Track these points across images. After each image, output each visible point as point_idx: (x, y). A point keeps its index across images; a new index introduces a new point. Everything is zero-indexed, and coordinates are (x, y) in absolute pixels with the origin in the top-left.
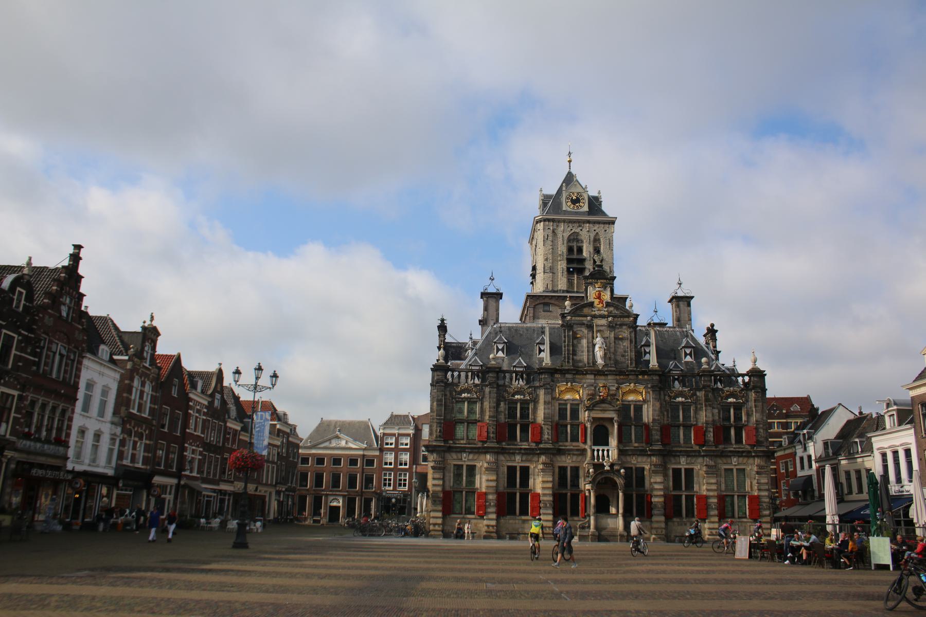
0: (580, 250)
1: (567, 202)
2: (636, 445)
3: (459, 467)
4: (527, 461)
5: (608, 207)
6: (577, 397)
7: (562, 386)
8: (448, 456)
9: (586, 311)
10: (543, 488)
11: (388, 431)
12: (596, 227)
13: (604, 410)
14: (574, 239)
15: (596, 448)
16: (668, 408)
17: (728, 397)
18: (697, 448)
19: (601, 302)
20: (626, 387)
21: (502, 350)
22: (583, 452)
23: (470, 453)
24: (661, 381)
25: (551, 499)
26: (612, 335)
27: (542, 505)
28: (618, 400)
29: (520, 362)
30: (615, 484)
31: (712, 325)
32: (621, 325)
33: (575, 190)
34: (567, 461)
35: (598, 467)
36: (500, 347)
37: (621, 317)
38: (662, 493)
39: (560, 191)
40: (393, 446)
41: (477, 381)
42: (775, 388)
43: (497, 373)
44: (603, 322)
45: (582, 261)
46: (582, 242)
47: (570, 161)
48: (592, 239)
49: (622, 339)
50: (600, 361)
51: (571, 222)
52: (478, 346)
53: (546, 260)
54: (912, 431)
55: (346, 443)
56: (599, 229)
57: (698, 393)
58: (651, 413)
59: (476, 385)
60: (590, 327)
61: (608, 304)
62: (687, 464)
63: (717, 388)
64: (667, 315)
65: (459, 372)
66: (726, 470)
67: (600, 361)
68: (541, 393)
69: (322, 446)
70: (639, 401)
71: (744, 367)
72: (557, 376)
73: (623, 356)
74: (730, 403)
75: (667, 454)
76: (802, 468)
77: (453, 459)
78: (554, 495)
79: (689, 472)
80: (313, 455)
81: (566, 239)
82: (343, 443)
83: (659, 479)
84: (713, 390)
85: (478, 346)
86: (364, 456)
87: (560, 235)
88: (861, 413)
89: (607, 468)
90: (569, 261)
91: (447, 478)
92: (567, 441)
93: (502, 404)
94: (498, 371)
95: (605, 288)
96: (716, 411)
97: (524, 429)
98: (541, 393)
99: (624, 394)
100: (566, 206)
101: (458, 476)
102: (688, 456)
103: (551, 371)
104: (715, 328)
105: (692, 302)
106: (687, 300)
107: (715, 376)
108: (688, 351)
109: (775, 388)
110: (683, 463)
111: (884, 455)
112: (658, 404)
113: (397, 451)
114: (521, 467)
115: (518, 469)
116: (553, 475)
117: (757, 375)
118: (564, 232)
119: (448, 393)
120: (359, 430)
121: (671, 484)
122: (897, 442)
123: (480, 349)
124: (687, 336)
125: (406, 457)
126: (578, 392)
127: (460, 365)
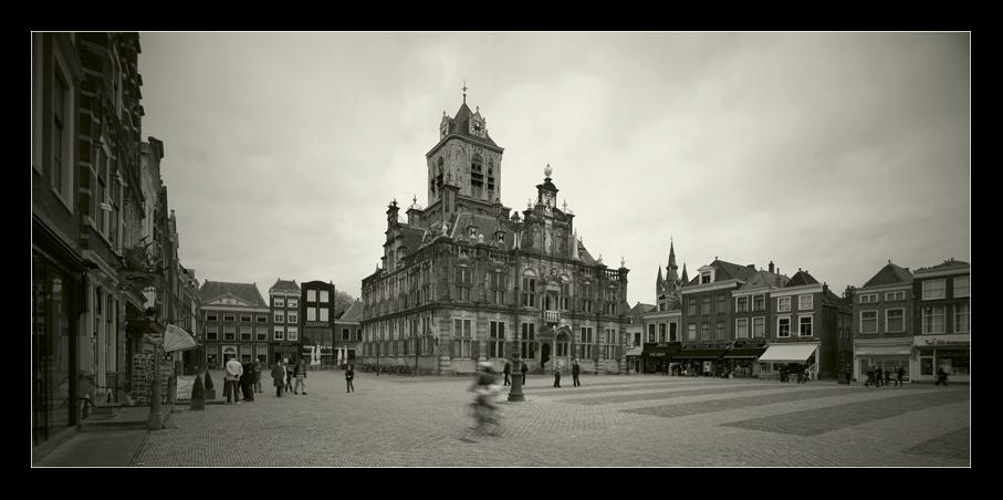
0: (479, 168)
3: (458, 322)
8: (451, 312)
13: (554, 285)
32: (560, 226)
34: (528, 320)
44: (548, 222)
45: (481, 177)
46: (481, 162)
50: (549, 252)
90: (473, 175)
92: (526, 304)
100: (472, 131)
101: (458, 327)
103: (521, 253)
110: (587, 324)
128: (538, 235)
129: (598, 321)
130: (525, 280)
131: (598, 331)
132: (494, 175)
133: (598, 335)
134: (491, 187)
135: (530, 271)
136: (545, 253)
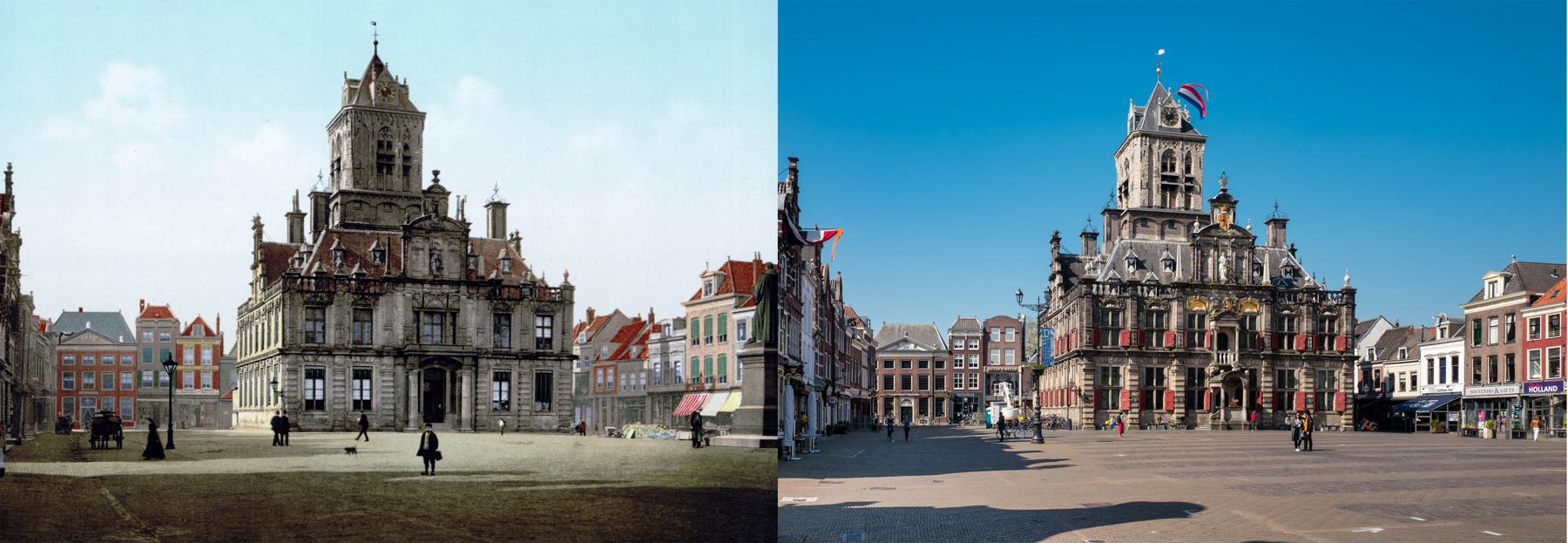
0: (1173, 168)
3: (1105, 369)
9: (1213, 232)
16: (1277, 320)
34: (1196, 363)
45: (1174, 178)
50: (1223, 277)
60: (1216, 247)
61: (1232, 227)
68: (1175, 305)
75: (1274, 358)
77: (1100, 363)
87: (1155, 151)
90: (1164, 178)
94: (1134, 284)
98: (1175, 305)
111: (1431, 361)
118: (1159, 148)
125: (976, 360)
134: (1189, 189)
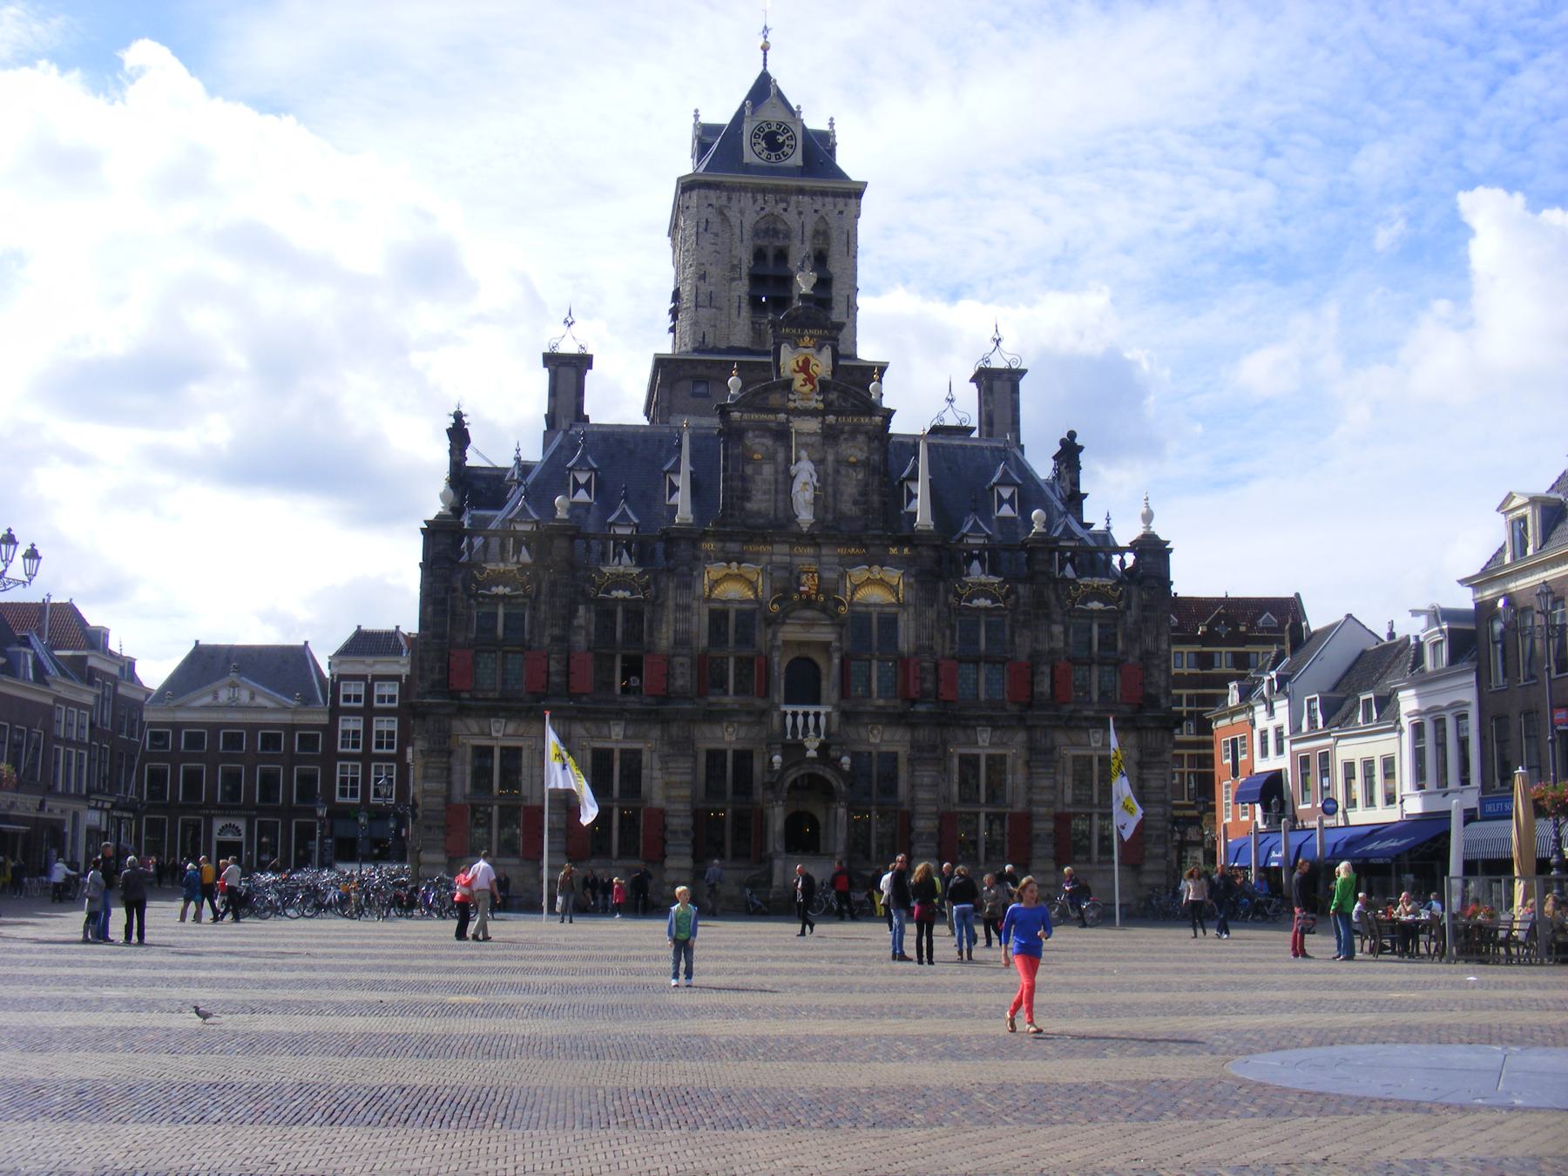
0: (782, 256)
1: (753, 145)
2: (881, 702)
3: (483, 753)
4: (635, 737)
5: (848, 160)
6: (750, 595)
7: (715, 571)
8: (457, 725)
9: (775, 399)
10: (668, 799)
11: (348, 669)
12: (819, 200)
13: (810, 624)
14: (767, 232)
15: (789, 709)
17: (1085, 601)
18: (1013, 709)
19: (810, 379)
20: (859, 574)
21: (587, 486)
22: (762, 715)
23: (509, 719)
24: (936, 563)
25: (690, 821)
26: (830, 458)
27: (668, 836)
28: (842, 603)
29: (624, 516)
30: (828, 793)
31: (1072, 435)
32: (855, 431)
33: (770, 114)
34: (728, 737)
35: (794, 750)
36: (582, 478)
37: (853, 414)
38: (934, 809)
39: (739, 117)
40: (361, 705)
41: (525, 557)
42: (1191, 577)
43: (572, 538)
44: (812, 425)
46: (787, 236)
47: (765, 49)
48: (809, 231)
49: (854, 465)
50: (805, 516)
51: (764, 190)
52: (530, 479)
53: (703, 277)
54: (1472, 678)
55: (252, 698)
56: (828, 206)
57: (1021, 589)
58: (912, 633)
59: (525, 567)
61: (824, 387)
62: (992, 745)
63: (1065, 579)
64: (967, 409)
65: (486, 538)
66: (1076, 759)
67: (805, 516)
69: (198, 703)
70: (890, 605)
71: (1125, 533)
72: (709, 546)
73: (855, 503)
74: (1092, 611)
76: (1264, 753)
78: (696, 814)
79: (996, 763)
80: (177, 727)
81: (748, 226)
82: (244, 697)
83: (926, 775)
84: (1056, 581)
85: (530, 479)
86: (291, 728)
88: (1391, 635)
89: (812, 753)
90: (756, 280)
91: (456, 777)
92: (726, 693)
93: (582, 610)
95: (820, 350)
96: (1057, 629)
97: (633, 667)
99: (856, 588)
102: (995, 728)
104: (1078, 441)
105: (1022, 383)
106: (1013, 377)
107: (1062, 551)
108: (1006, 493)
109: (1191, 577)
112: (931, 614)
113: (369, 713)
114: (623, 752)
115: (617, 755)
116: (694, 770)
117: (1153, 551)
118: (746, 212)
119: (459, 585)
120: (281, 667)
121: (955, 789)
122: (1443, 701)
123: (535, 484)
124: (1006, 460)
126: (752, 585)
127: (488, 520)
128: (768, 470)
129: (1030, 729)
130: (718, 618)
131: (1028, 763)
132: (835, 267)
133: (1030, 776)
135: (731, 585)
136: (792, 518)
